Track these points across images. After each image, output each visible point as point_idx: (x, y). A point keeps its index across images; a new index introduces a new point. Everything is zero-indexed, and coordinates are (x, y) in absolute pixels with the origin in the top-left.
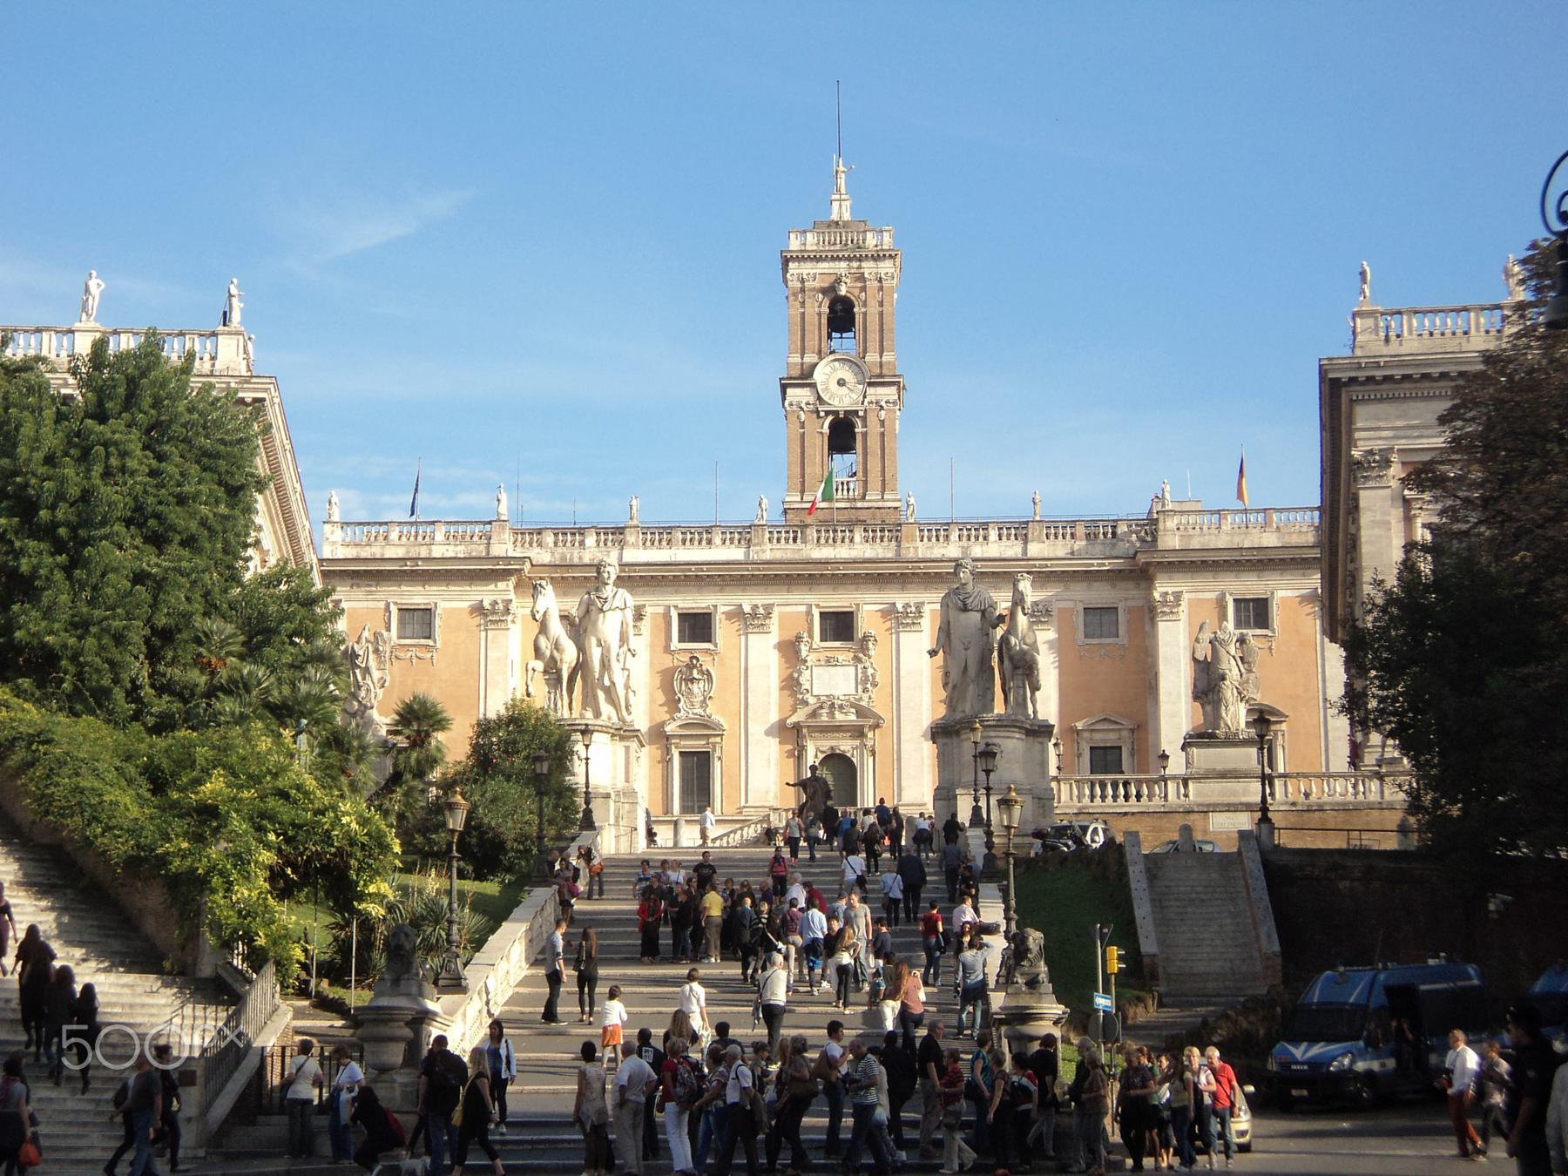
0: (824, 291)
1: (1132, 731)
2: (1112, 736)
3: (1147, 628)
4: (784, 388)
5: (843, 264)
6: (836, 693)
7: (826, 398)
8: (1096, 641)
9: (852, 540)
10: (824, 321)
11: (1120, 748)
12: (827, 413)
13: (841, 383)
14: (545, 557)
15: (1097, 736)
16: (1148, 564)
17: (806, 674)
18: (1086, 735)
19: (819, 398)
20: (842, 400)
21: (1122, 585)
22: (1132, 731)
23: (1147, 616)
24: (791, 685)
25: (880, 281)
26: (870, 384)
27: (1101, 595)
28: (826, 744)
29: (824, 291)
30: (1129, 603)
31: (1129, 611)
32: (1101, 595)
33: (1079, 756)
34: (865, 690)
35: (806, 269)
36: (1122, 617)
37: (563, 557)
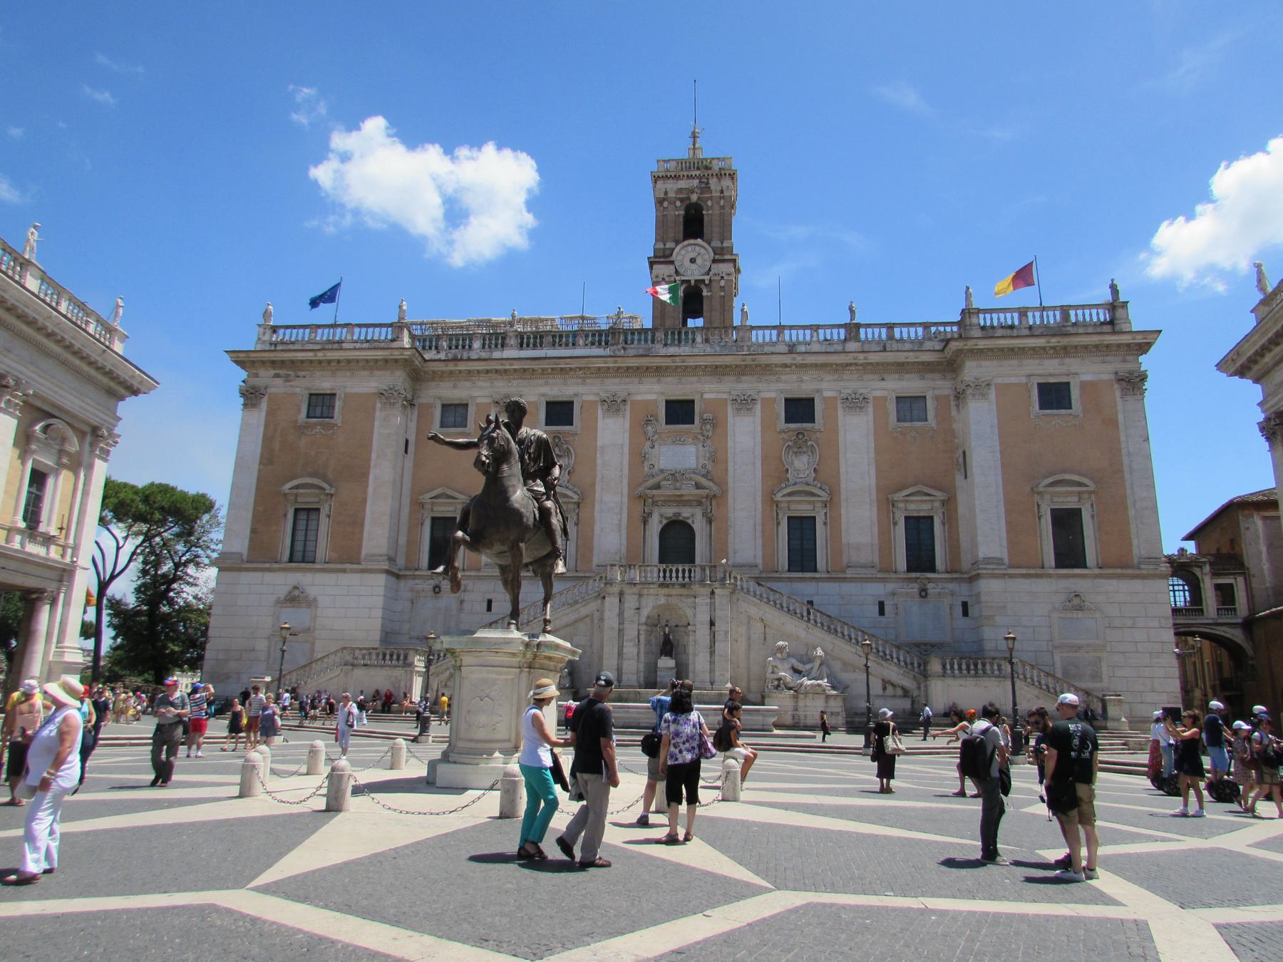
0: (682, 200)
1: (943, 503)
2: (926, 506)
3: (954, 413)
4: (651, 264)
5: (696, 182)
6: (679, 467)
7: (681, 271)
8: (907, 424)
9: (694, 341)
10: (681, 220)
11: (932, 518)
12: (683, 282)
13: (693, 261)
14: (442, 356)
15: (912, 507)
16: (961, 350)
17: (655, 451)
18: (901, 505)
19: (677, 272)
20: (693, 273)
21: (929, 376)
22: (943, 503)
23: (953, 403)
24: (638, 457)
25: (722, 192)
26: (714, 261)
27: (912, 385)
28: (670, 511)
29: (682, 200)
30: (937, 392)
31: (937, 398)
32: (912, 385)
33: (895, 524)
34: (704, 466)
35: (672, 186)
36: (930, 403)
37: (455, 355)
